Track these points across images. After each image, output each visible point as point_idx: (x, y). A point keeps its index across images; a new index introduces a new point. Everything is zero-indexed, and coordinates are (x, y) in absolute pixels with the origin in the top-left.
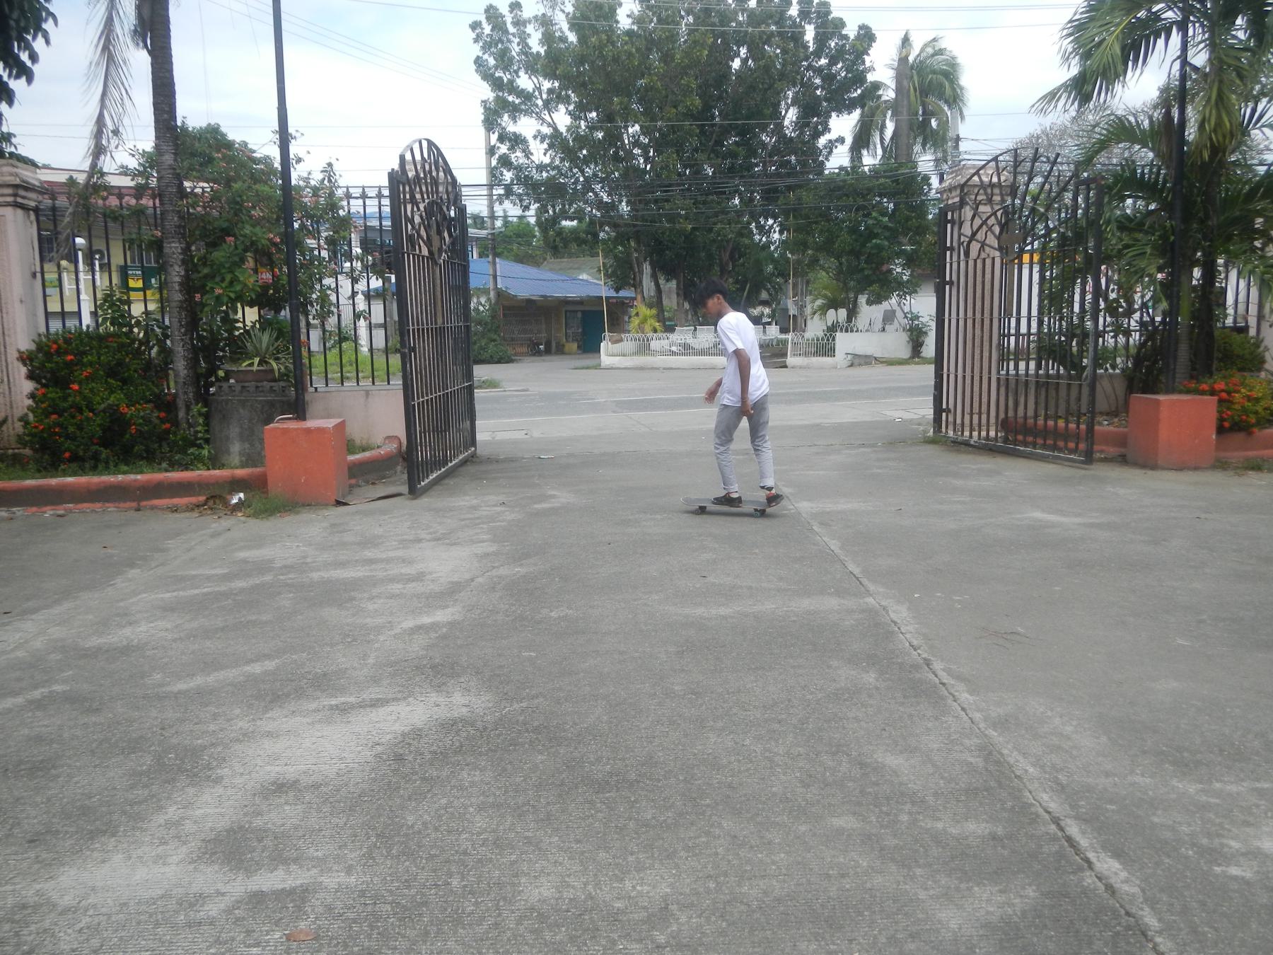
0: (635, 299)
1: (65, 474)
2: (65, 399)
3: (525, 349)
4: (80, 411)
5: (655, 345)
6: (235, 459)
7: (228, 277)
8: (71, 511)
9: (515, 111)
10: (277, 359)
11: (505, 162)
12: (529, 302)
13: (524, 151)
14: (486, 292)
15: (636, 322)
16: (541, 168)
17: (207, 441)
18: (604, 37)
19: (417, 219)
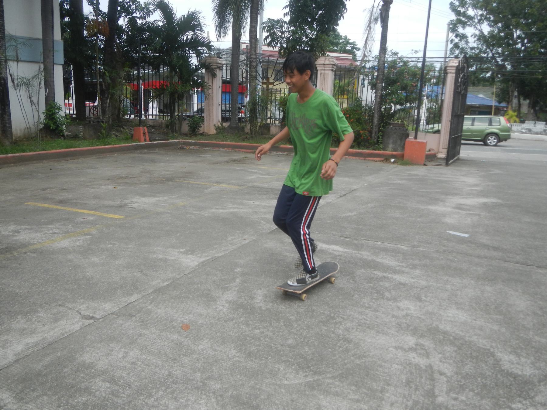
9: (464, 24)
11: (456, 46)
16: (472, 49)
17: (381, 143)
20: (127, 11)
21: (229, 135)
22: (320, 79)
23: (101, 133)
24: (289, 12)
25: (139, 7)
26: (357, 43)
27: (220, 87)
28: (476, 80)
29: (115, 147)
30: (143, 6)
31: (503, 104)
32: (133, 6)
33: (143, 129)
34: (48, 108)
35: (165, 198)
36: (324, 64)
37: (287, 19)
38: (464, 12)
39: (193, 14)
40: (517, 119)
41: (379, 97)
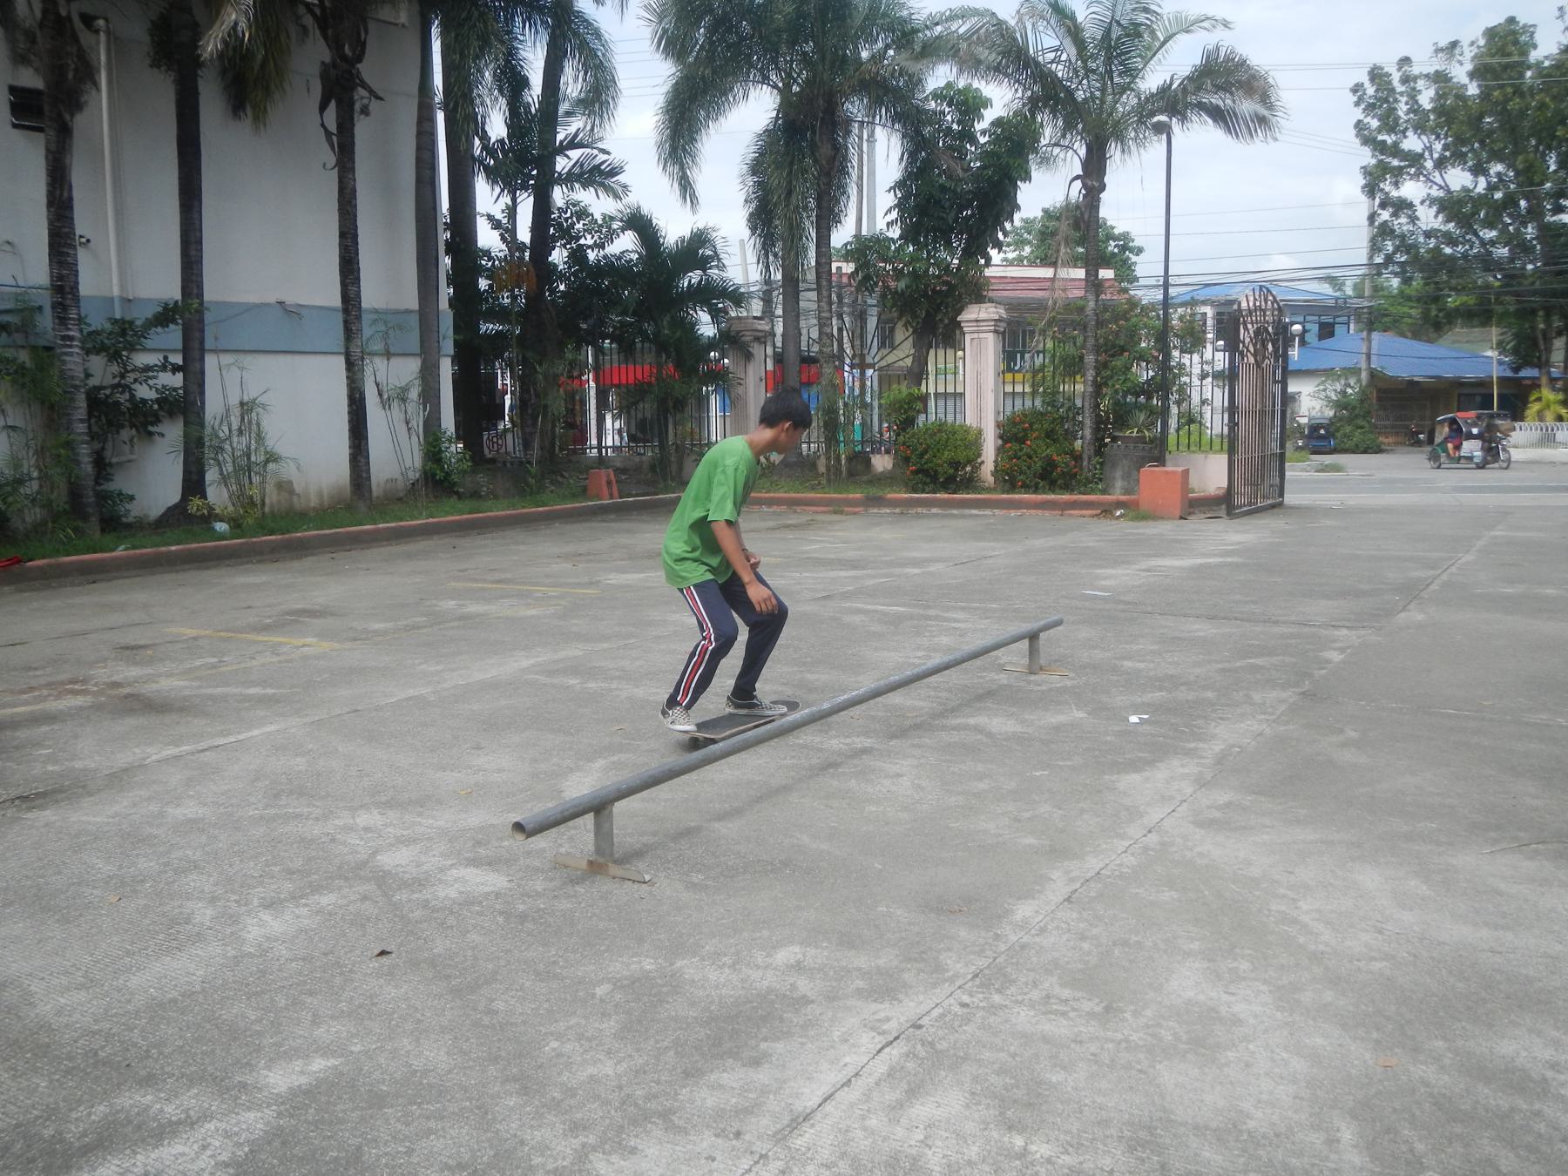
0: (1538, 378)
2: (1021, 450)
3: (1400, 439)
6: (1118, 491)
7: (1122, 378)
8: (1024, 513)
9: (1398, 173)
10: (1148, 430)
11: (1385, 231)
12: (1412, 384)
13: (1410, 217)
14: (1355, 371)
15: (1534, 408)
16: (1428, 234)
17: (1101, 480)
18: (1509, 90)
19: (1247, 340)
20: (567, 234)
21: (783, 479)
22: (971, 351)
23: (528, 484)
24: (897, 219)
26: (1133, 235)
27: (761, 380)
28: (1441, 315)
30: (600, 222)
32: (577, 226)
33: (604, 474)
34: (431, 440)
36: (977, 321)
37: (895, 233)
38: (1396, 144)
41: (1090, 383)
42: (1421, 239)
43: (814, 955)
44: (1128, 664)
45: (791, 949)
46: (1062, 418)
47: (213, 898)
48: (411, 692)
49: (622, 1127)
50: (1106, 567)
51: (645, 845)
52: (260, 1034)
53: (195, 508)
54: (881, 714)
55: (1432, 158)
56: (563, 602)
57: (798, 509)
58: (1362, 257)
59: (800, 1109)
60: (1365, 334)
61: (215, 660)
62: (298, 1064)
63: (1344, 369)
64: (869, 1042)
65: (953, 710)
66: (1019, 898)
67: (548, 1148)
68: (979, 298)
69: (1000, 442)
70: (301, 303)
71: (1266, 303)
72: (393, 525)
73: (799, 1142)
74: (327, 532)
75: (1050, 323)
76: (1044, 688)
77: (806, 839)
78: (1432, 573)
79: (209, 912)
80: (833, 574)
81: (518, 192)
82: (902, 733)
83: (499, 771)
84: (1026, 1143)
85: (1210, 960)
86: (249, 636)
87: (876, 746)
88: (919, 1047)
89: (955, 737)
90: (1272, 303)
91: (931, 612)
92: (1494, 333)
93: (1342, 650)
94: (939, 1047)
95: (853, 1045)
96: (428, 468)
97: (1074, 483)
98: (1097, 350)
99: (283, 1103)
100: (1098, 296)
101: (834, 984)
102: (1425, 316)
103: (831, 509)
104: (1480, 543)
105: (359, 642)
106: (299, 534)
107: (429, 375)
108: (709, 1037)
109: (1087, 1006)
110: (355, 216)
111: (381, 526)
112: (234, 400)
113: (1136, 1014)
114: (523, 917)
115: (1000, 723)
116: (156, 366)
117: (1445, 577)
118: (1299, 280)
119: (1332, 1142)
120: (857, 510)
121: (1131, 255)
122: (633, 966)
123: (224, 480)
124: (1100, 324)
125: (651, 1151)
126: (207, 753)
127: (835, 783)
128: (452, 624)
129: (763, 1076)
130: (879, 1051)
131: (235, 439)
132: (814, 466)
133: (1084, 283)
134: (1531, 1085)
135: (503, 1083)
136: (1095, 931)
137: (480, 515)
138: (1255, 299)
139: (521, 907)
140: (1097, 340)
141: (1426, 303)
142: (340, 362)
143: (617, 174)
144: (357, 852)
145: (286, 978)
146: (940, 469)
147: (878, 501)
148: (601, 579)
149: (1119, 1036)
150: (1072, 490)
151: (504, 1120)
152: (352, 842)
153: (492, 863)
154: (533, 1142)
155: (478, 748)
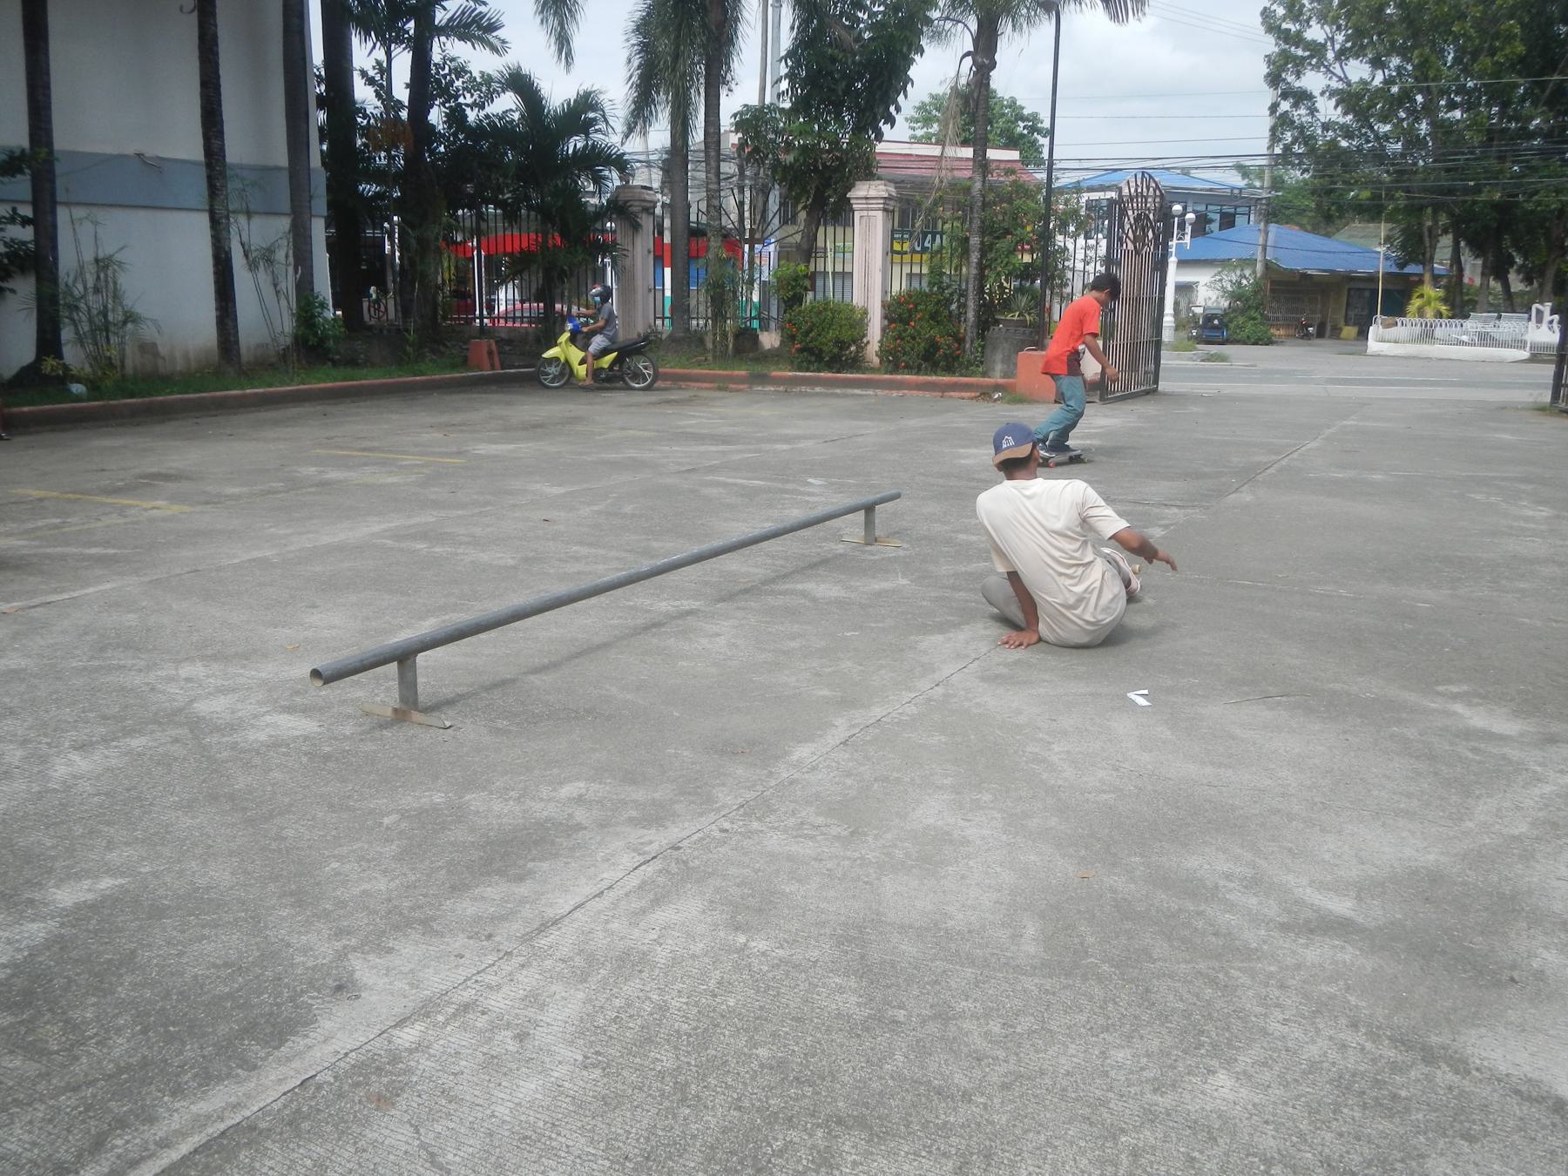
0: (1422, 275)
1: (903, 374)
2: (905, 330)
3: (1291, 331)
4: (914, 338)
5: (1439, 332)
6: (998, 374)
9: (1299, 65)
10: (1029, 314)
11: (1282, 122)
12: (1305, 276)
13: (1309, 108)
14: (1251, 262)
15: (1416, 303)
16: (1326, 127)
17: (982, 362)
20: (447, 93)
21: (669, 354)
24: (787, 90)
25: (472, 86)
27: (649, 252)
28: (1333, 208)
29: (433, 380)
30: (479, 80)
31: (1412, 269)
32: (458, 83)
33: (485, 344)
34: (302, 304)
35: (530, 445)
38: (1299, 33)
39: (587, 95)
40: (1443, 308)
41: (974, 265)
42: (1319, 132)
43: (596, 790)
44: (962, 537)
45: (576, 784)
46: (947, 300)
47: (25, 740)
48: (256, 554)
49: (384, 932)
50: (969, 447)
51: (459, 695)
52: (54, 858)
53: (49, 368)
54: (714, 579)
55: (1333, 49)
56: (426, 471)
57: (683, 385)
58: (1262, 146)
59: (552, 916)
60: (1262, 225)
61: (59, 520)
62: (86, 883)
63: (1240, 260)
64: (627, 860)
65: (785, 576)
66: (800, 742)
67: (311, 949)
68: (869, 175)
69: (886, 322)
70: (161, 155)
71: (1148, 190)
72: (261, 390)
73: (543, 942)
74: (191, 396)
75: (935, 203)
76: (876, 557)
77: (614, 690)
78: (1275, 458)
79: (19, 753)
80: (702, 448)
81: (393, 45)
82: (730, 597)
83: (331, 627)
84: (748, 941)
85: (958, 793)
86: (98, 499)
87: (702, 608)
88: (673, 864)
89: (780, 601)
90: (1155, 191)
91: (789, 486)
92: (1383, 229)
93: (1166, 527)
94: (691, 864)
95: (614, 864)
96: (300, 333)
97: (956, 364)
98: (983, 231)
99: (66, 916)
100: (984, 177)
101: (609, 814)
102: (1319, 205)
103: (716, 385)
104: (1328, 432)
105: (209, 506)
106: (160, 398)
107: (300, 236)
108: (481, 858)
109: (835, 831)
110: (217, 64)
111: (248, 391)
112: (88, 256)
113: (876, 837)
114: (327, 758)
115: (825, 589)
116: (5, 218)
117: (1284, 462)
118: (1197, 168)
119: (1016, 937)
120: (741, 387)
121: (1039, 137)
122: (423, 800)
123: (80, 340)
124: (985, 205)
125: (407, 950)
126: (38, 609)
127: (655, 641)
128: (310, 490)
129: (523, 890)
130: (636, 868)
131: (91, 297)
132: (701, 341)
133: (971, 163)
134: (1204, 891)
135: (279, 897)
136: (862, 769)
137: (354, 383)
138: (1137, 185)
139: (328, 749)
140: (983, 222)
141: (1319, 196)
142: (204, 219)
143: (496, 29)
144: (174, 700)
145: (86, 811)
146: (825, 348)
147: (763, 379)
148: (470, 448)
149: (857, 855)
150: (954, 373)
151: (275, 927)
152: (172, 691)
153: (305, 711)
154: (298, 946)
155: (314, 606)
